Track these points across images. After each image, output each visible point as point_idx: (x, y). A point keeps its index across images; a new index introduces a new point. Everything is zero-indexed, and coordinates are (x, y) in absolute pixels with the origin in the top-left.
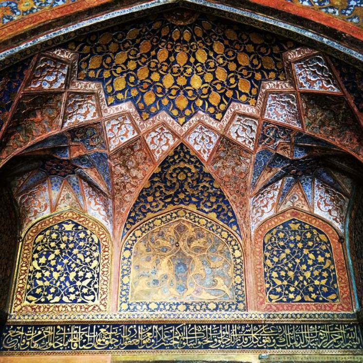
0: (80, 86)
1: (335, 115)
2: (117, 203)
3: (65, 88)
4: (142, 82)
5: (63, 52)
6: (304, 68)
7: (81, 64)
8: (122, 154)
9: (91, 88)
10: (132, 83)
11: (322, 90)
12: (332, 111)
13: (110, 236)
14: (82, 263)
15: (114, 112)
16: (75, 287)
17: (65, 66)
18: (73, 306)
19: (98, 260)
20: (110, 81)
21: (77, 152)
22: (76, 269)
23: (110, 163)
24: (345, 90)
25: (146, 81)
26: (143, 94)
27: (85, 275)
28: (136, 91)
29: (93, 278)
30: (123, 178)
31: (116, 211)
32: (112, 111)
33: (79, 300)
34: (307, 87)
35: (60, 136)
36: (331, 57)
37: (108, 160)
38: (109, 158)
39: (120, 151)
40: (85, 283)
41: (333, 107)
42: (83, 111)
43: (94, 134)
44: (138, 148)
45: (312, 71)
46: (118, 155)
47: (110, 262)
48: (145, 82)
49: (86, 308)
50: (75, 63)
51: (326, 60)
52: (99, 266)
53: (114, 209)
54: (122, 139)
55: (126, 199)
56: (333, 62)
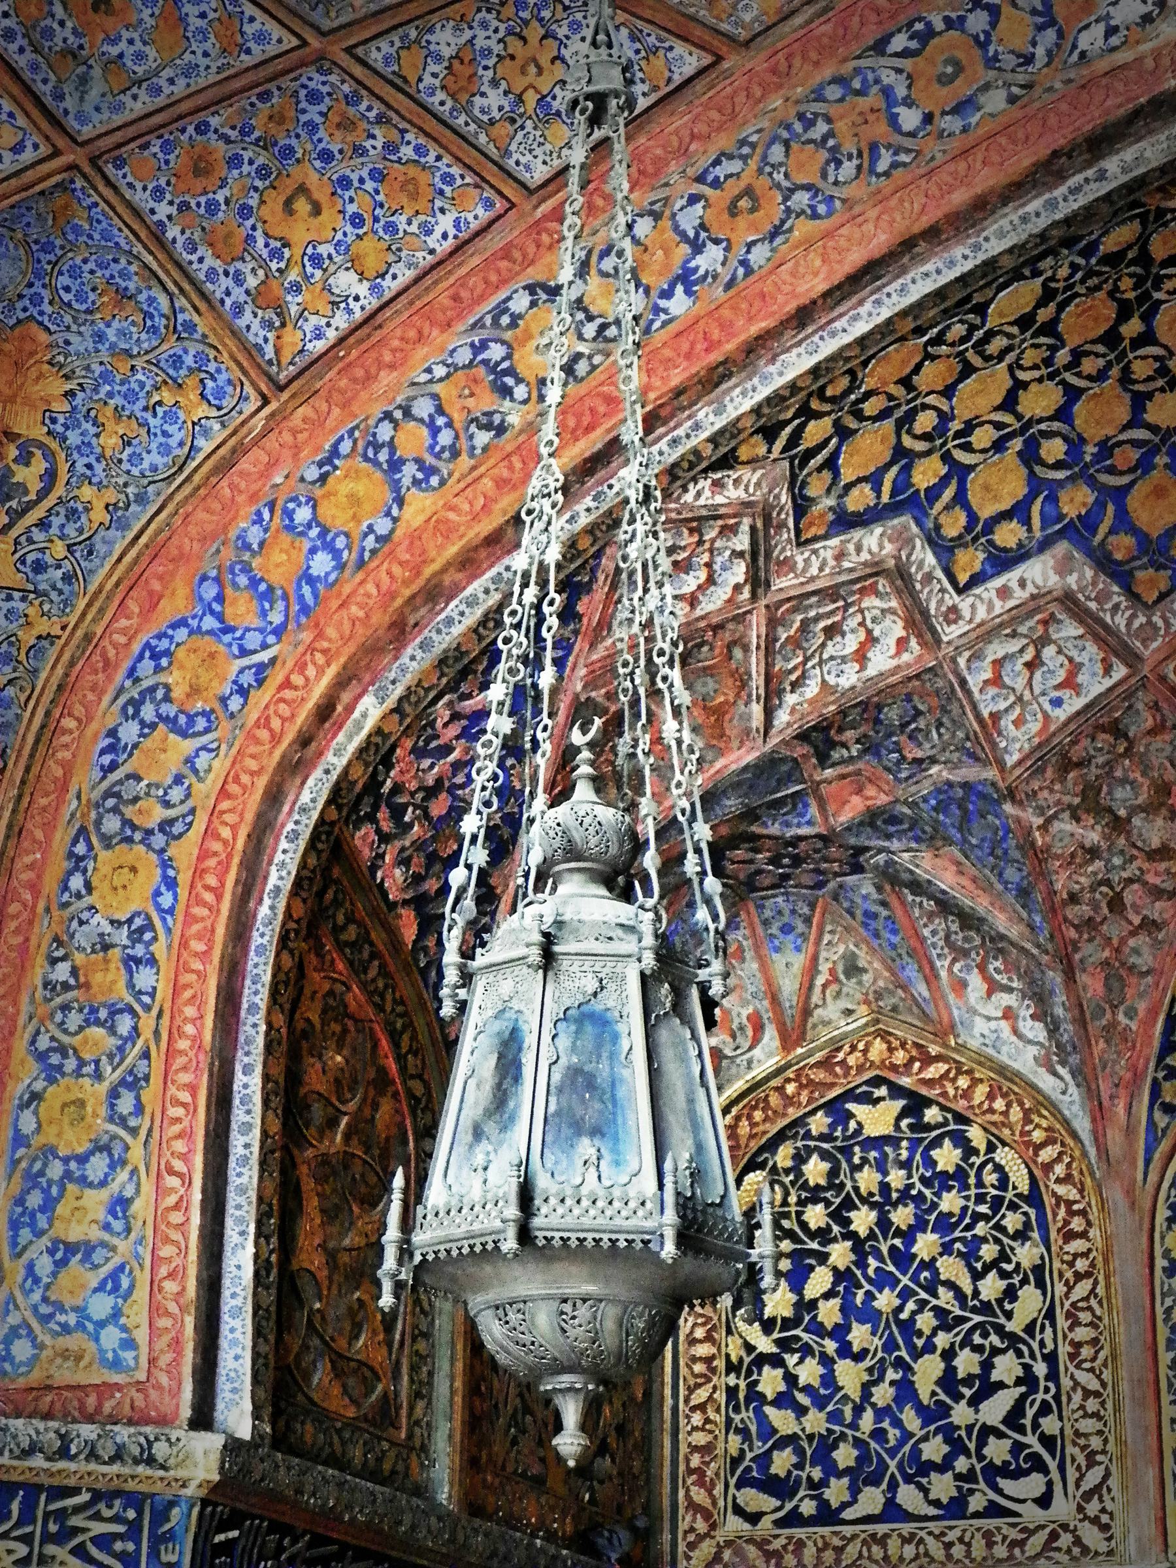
0: (813, 564)
2: (1092, 985)
3: (754, 596)
4: (1106, 448)
5: (718, 485)
7: (804, 484)
8: (1066, 765)
9: (865, 556)
10: (1058, 465)
13: (1085, 1154)
14: (963, 1306)
15: (990, 607)
16: (949, 1433)
17: (738, 524)
18: (952, 1536)
19: (1041, 1285)
20: (948, 493)
21: (856, 800)
22: (942, 1340)
23: (1018, 820)
25: (1122, 437)
26: (1121, 493)
27: (987, 1366)
28: (1086, 489)
29: (1028, 1380)
30: (1098, 864)
31: (1094, 1027)
32: (984, 604)
33: (976, 1503)
35: (769, 769)
37: (1008, 808)
38: (1011, 794)
39: (1055, 756)
40: (995, 1410)
42: (851, 643)
43: (919, 713)
44: (1150, 723)
46: (1049, 774)
47: (1100, 1290)
48: (1120, 444)
49: (1014, 1544)
50: (777, 497)
52: (1050, 1315)
53: (1081, 1022)
54: (1057, 703)
55: (1133, 960)
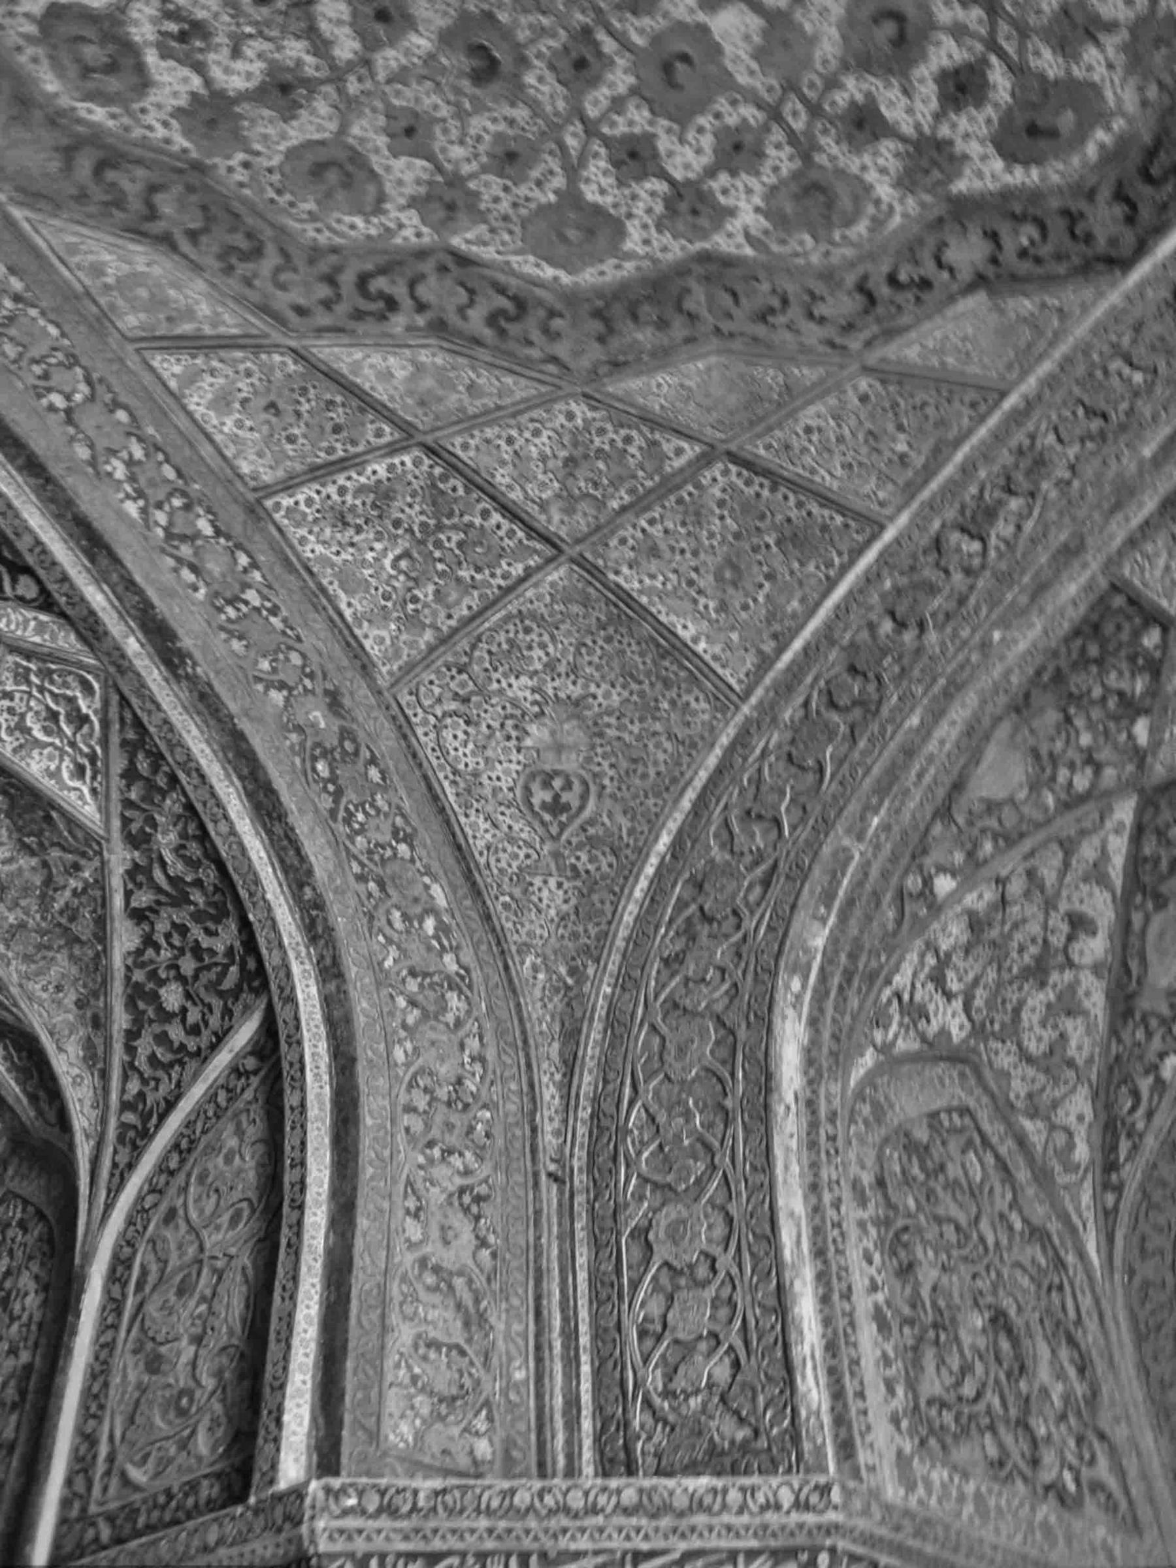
1: (48, 881)
6: (29, 683)
11: (48, 785)
12: (45, 864)
24: (116, 823)
34: (9, 748)
36: (124, 701)
41: (55, 853)
45: (48, 708)
51: (106, 703)
56: (122, 720)
